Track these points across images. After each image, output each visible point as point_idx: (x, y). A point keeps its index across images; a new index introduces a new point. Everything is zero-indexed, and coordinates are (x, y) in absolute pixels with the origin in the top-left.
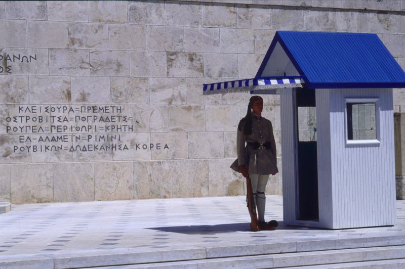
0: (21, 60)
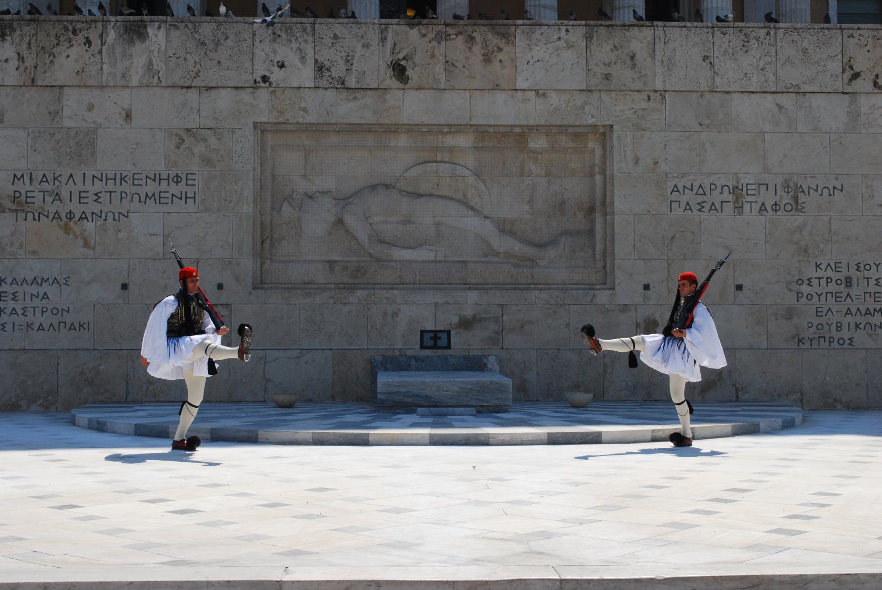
0: (820, 192)
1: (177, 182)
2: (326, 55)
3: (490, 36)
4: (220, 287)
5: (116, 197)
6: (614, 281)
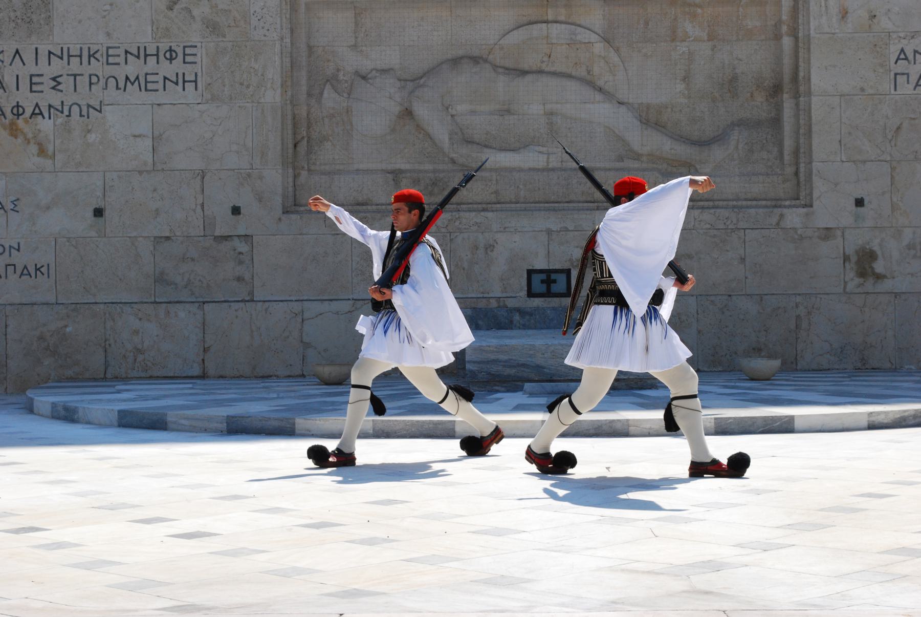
1: (171, 59)
4: (236, 211)
5: (83, 81)
6: (811, 194)
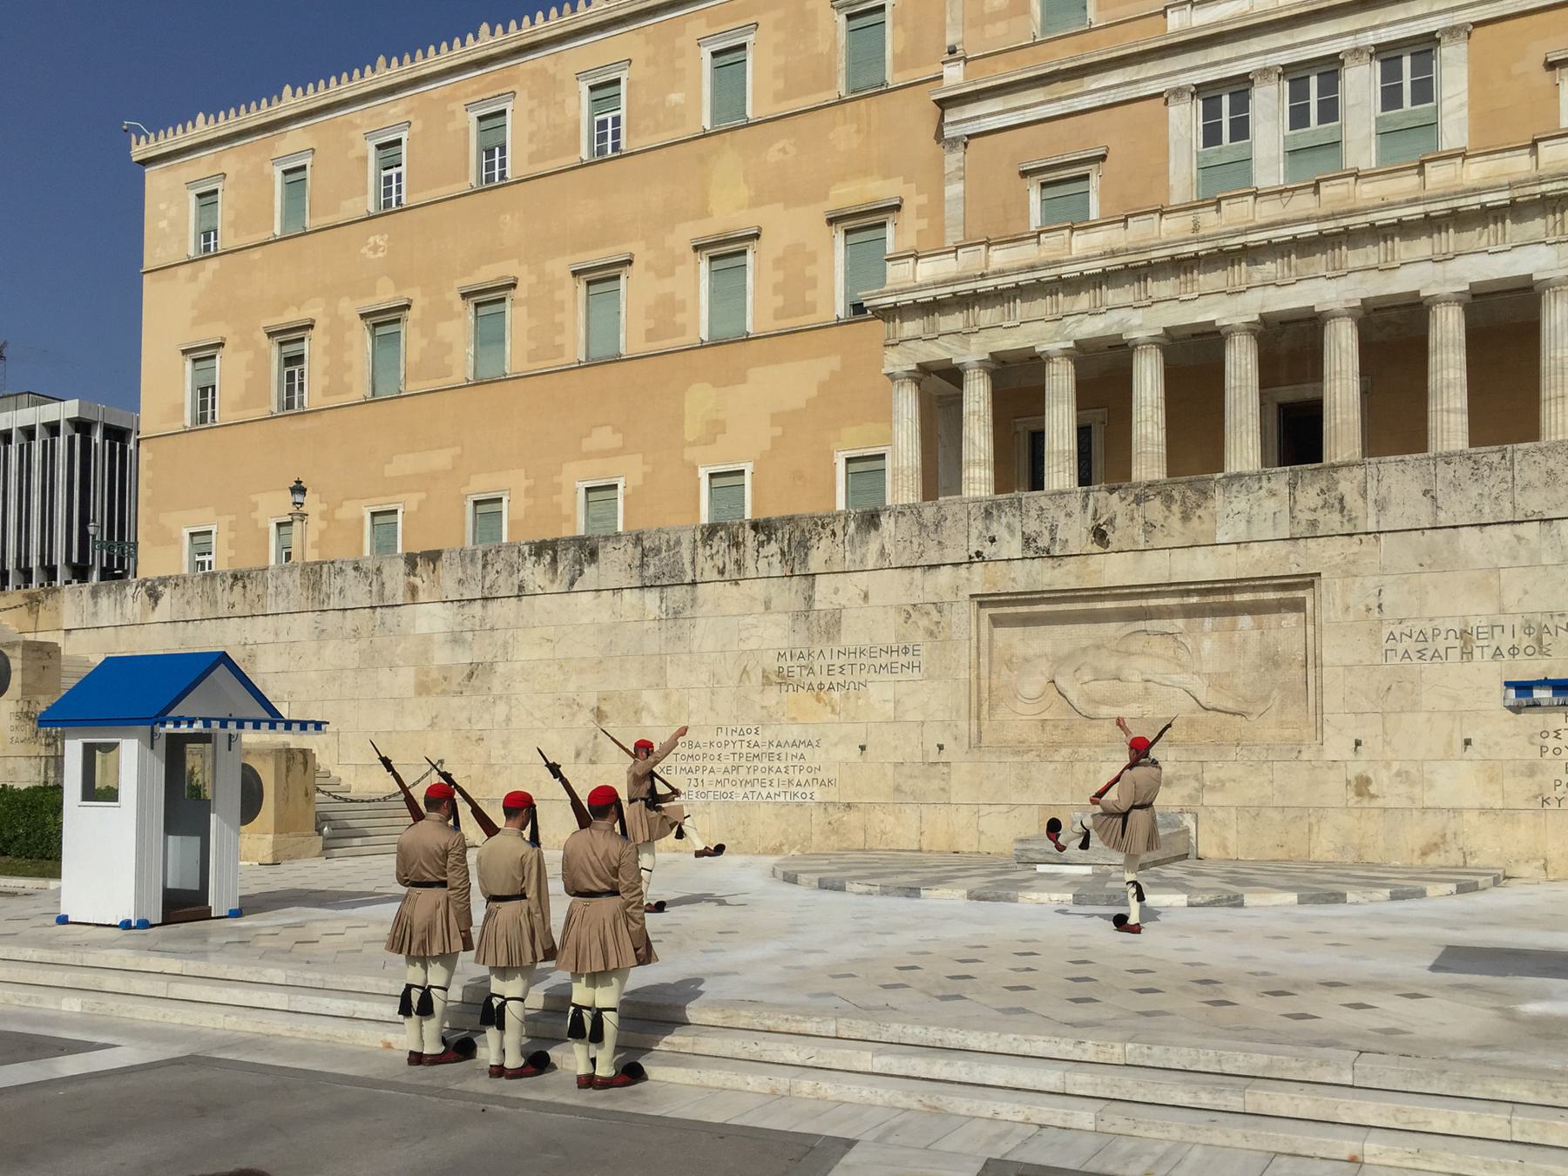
2: (1032, 526)
3: (1189, 493)
4: (941, 747)
